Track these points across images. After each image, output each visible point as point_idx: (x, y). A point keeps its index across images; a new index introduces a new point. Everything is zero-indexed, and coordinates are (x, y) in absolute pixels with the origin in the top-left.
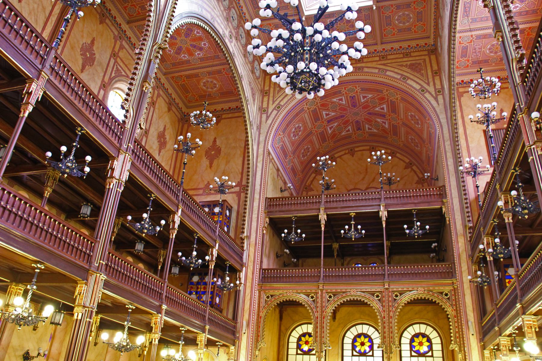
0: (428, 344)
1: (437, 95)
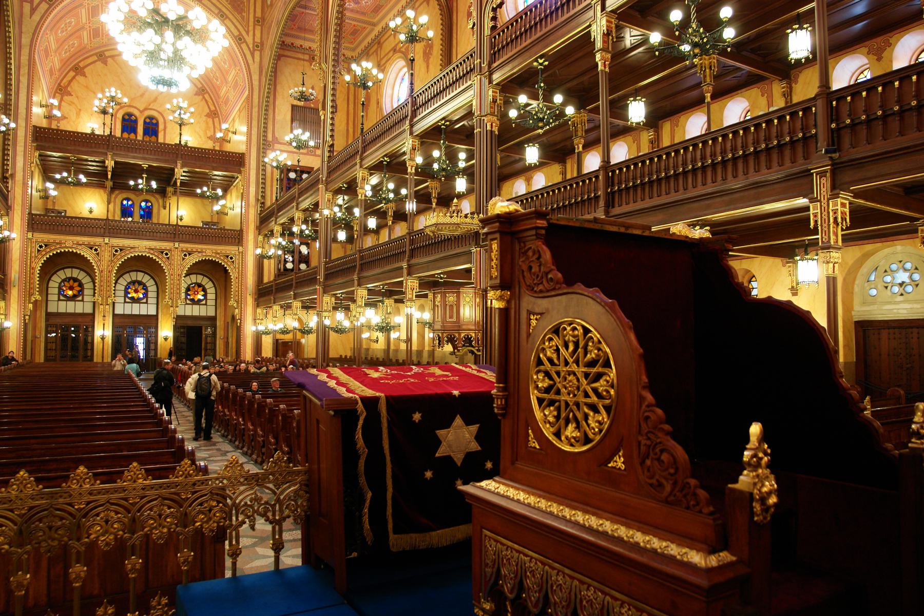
0: (202, 293)
1: (254, 50)
